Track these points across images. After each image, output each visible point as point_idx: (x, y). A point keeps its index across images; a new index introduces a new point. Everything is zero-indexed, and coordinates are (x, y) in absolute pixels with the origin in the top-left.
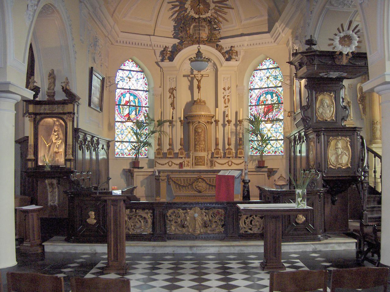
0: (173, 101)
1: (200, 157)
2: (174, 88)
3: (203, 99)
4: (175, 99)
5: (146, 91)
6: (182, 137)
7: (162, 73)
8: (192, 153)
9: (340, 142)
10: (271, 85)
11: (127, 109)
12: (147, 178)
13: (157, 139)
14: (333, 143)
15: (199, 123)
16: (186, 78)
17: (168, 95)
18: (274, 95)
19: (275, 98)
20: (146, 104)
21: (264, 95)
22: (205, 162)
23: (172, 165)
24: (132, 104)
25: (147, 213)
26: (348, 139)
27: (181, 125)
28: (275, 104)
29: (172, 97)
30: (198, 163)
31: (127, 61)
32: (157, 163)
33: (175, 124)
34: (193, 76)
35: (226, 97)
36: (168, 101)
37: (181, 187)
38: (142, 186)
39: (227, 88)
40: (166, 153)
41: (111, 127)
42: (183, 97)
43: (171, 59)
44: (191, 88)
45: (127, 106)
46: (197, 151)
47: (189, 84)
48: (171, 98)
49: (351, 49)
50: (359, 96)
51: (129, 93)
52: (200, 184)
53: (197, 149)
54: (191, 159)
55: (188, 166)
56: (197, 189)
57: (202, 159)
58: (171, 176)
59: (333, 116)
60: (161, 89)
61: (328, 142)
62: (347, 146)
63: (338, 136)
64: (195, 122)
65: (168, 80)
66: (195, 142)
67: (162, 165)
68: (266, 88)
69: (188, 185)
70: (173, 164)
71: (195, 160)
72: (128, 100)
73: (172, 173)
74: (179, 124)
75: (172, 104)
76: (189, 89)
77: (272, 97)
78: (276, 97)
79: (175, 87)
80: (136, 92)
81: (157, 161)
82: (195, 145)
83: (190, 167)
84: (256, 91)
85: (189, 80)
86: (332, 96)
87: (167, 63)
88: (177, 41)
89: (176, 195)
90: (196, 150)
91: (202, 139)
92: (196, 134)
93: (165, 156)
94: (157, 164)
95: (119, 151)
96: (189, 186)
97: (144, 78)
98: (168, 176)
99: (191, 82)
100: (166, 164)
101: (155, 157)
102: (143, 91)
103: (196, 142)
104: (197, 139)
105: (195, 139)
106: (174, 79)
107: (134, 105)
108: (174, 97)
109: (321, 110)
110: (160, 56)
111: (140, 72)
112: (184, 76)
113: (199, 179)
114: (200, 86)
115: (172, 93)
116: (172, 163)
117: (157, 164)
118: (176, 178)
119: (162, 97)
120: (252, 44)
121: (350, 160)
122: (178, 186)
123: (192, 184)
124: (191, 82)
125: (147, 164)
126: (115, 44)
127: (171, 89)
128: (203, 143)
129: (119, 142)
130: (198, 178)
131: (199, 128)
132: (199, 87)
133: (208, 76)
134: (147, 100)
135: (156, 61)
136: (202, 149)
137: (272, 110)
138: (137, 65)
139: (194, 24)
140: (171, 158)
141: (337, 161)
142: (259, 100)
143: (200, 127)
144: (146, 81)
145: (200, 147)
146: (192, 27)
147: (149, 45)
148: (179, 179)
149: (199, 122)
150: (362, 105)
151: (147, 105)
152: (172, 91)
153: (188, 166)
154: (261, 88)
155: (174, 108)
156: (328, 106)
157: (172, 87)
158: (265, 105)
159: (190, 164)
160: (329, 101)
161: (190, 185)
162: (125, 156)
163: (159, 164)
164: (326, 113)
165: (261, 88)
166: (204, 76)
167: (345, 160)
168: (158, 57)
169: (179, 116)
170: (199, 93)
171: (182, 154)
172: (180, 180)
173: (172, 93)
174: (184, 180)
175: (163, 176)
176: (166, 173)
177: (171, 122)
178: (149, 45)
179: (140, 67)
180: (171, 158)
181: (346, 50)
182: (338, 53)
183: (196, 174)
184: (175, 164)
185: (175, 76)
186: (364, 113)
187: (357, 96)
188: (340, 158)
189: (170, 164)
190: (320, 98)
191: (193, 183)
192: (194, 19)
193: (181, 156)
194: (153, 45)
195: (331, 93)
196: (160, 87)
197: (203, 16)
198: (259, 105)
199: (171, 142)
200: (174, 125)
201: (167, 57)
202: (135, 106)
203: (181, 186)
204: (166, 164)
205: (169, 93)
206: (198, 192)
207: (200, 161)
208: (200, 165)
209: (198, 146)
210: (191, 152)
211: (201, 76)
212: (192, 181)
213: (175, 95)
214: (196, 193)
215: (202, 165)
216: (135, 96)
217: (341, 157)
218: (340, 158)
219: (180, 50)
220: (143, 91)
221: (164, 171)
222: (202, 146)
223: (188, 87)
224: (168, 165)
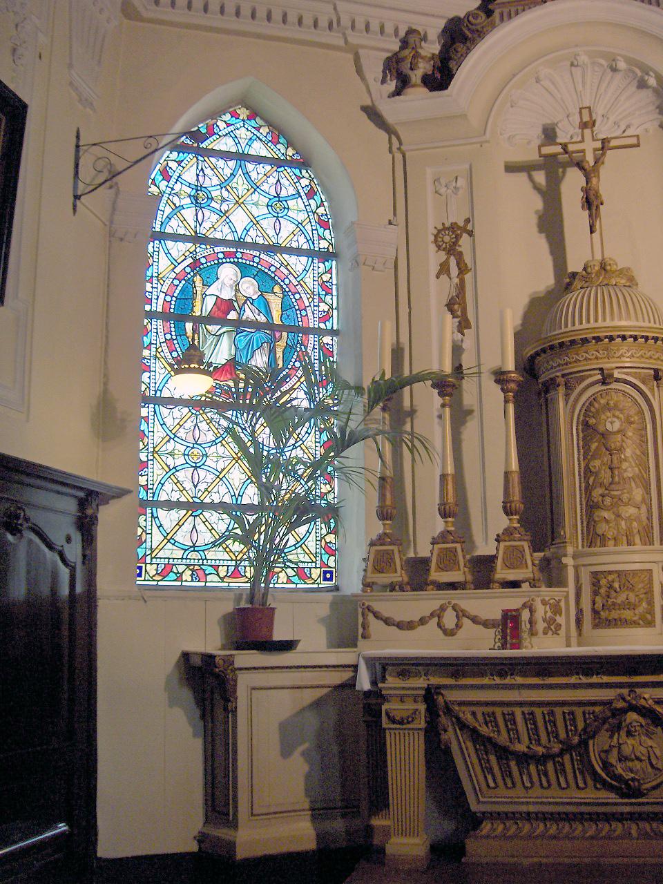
0: (461, 287)
1: (619, 573)
2: (461, 224)
3: (620, 257)
4: (468, 277)
5: (325, 256)
6: (514, 466)
7: (399, 156)
8: (574, 557)
11: (225, 338)
12: (317, 704)
13: (376, 483)
15: (604, 382)
16: (523, 176)
17: (435, 258)
20: (326, 317)
22: (651, 603)
23: (458, 626)
24: (248, 314)
27: (506, 401)
29: (454, 271)
30: (614, 614)
31: (227, 117)
32: (377, 615)
33: (476, 408)
34: (558, 149)
36: (436, 291)
37: (513, 764)
38: (286, 752)
40: (425, 562)
41: (115, 419)
42: (513, 271)
43: (440, 79)
44: (551, 224)
45: (224, 322)
46: (604, 540)
47: (538, 203)
48: (448, 273)
51: (234, 263)
52: (629, 745)
53: (602, 528)
54: (571, 588)
55: (556, 633)
56: (618, 778)
57: (632, 589)
58: (453, 696)
60: (397, 232)
64: (583, 379)
65: (430, 188)
66: (588, 490)
67: (400, 626)
69: (556, 748)
70: (466, 622)
71: (595, 593)
72: (227, 294)
73: (455, 675)
74: (494, 394)
75: (455, 305)
76: (541, 231)
79: (467, 221)
80: (275, 260)
81: (377, 606)
82: (591, 507)
83: (568, 638)
85: (536, 187)
87: (418, 99)
89: (483, 808)
90: (593, 538)
91: (629, 469)
92: (594, 446)
93: (418, 576)
94: (375, 625)
95: (179, 554)
96: (567, 758)
97: (311, 194)
98: (429, 696)
99: (551, 197)
100: (423, 621)
101: (367, 585)
102: (310, 253)
103: (597, 492)
104: (597, 474)
105: (588, 472)
106: (462, 182)
107: (262, 319)
108: (463, 269)
110: (383, 81)
112: (511, 168)
113: (624, 711)
114: (597, 195)
115: (452, 250)
116: (461, 614)
117: (375, 625)
118: (479, 710)
119: (401, 271)
122: (493, 758)
123: (584, 743)
124: (551, 197)
125: (322, 621)
126: (145, 14)
127: (444, 229)
128: (638, 494)
129: (178, 505)
130: (621, 704)
131: (607, 407)
132: (591, 202)
133: (634, 141)
134: (332, 300)
135: (368, 102)
136: (629, 528)
138: (278, 132)
140: (452, 586)
143: (616, 407)
144: (321, 211)
145: (618, 516)
147: (323, 23)
148: (498, 711)
149: (606, 379)
151: (334, 323)
152: (452, 239)
153: (556, 633)
155: (463, 325)
157: (452, 220)
159: (566, 620)
161: (567, 748)
162: (213, 581)
163: (387, 621)
166: (613, 143)
168: (375, 86)
169: (491, 362)
170: (592, 232)
171: (515, 560)
172: (510, 720)
173: (452, 250)
174: (530, 718)
175: (402, 701)
176: (418, 675)
177: (447, 386)
178: (323, 23)
179: (289, 144)
180: (452, 586)
183: (606, 679)
184: (475, 620)
185: (467, 166)
189: (449, 619)
191: (589, 734)
193: (511, 575)
194: (346, 22)
196: (390, 223)
199: (451, 499)
200: (470, 412)
201: (416, 77)
202: (269, 326)
203: (514, 753)
204: (423, 621)
205: (439, 247)
206: (623, 796)
207: (621, 598)
208: (626, 623)
209: (605, 514)
210: (570, 550)
211: (599, 145)
212: (581, 725)
213: (468, 259)
214: (612, 797)
215: (634, 624)
216: (266, 279)
219: (480, 34)
220: (310, 253)
221: (406, 667)
222: (632, 511)
223: (534, 220)
224: (439, 626)
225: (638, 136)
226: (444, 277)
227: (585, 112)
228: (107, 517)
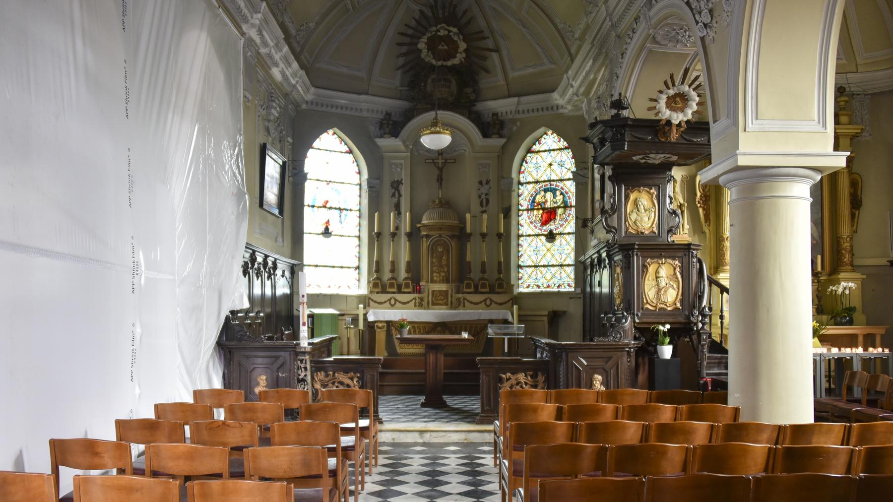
10: (554, 177)
14: (651, 269)
18: (558, 193)
19: (559, 198)
21: (542, 193)
25: (352, 379)
26: (677, 262)
28: (559, 207)
35: (483, 196)
39: (484, 182)
49: (685, 115)
50: (699, 194)
62: (675, 274)
63: (660, 257)
68: (545, 181)
77: (555, 196)
78: (561, 197)
84: (530, 187)
86: (652, 194)
100: (385, 302)
109: (634, 217)
111: (347, 152)
116: (396, 300)
117: (372, 303)
120: (526, 110)
121: (680, 297)
137: (555, 218)
139: (434, 76)
140: (394, 293)
141: (658, 298)
142: (534, 201)
146: (429, 81)
150: (704, 209)
154: (537, 182)
156: (645, 211)
158: (542, 209)
163: (375, 302)
164: (642, 221)
165: (537, 182)
167: (672, 297)
181: (677, 118)
182: (663, 122)
184: (400, 302)
186: (706, 222)
187: (696, 195)
189: (393, 302)
190: (632, 197)
192: (432, 68)
197: (449, 63)
198: (532, 210)
204: (385, 302)
217: (665, 292)
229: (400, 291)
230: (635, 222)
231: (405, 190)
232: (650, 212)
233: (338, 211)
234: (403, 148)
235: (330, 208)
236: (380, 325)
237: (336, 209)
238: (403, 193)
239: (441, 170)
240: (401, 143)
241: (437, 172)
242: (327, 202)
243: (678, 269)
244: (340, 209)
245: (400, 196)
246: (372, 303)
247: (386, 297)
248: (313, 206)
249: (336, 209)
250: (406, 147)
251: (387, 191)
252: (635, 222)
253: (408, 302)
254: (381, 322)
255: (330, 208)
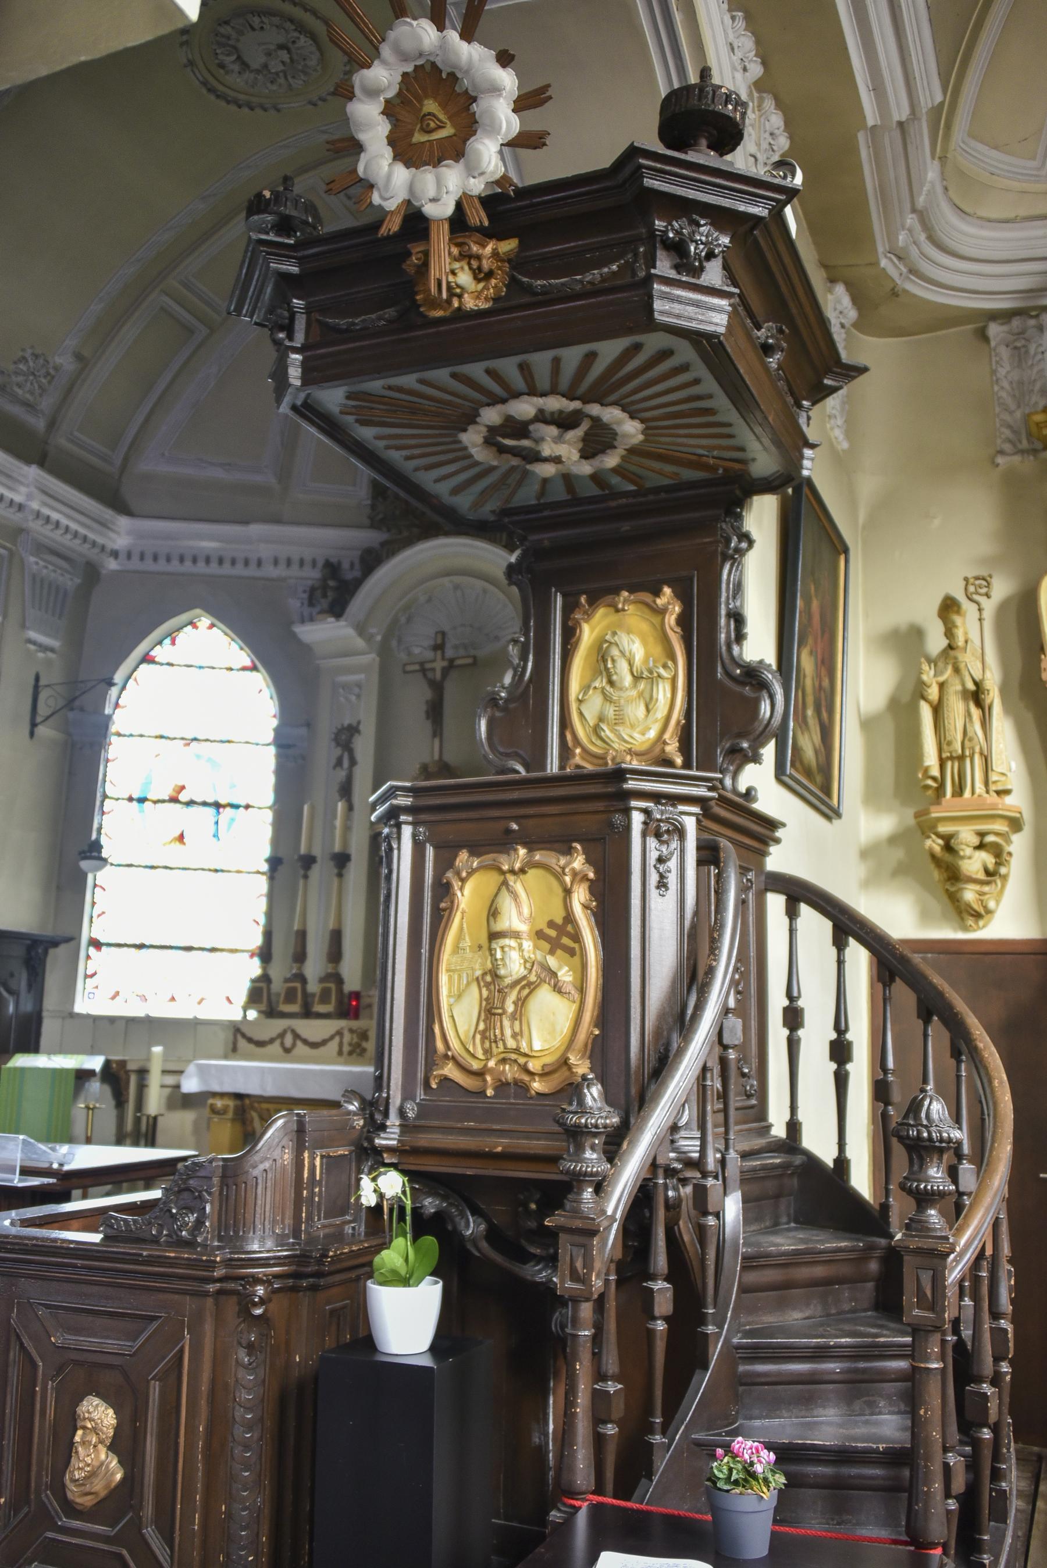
9: (519, 887)
14: (468, 896)
23: (294, 1045)
26: (578, 862)
29: (346, 763)
32: (244, 1036)
59: (667, 736)
61: (443, 890)
62: (569, 918)
63: (505, 843)
70: (299, 1043)
86: (662, 612)
88: (371, 537)
100: (272, 1041)
116: (296, 1036)
156: (637, 678)
160: (645, 643)
164: (619, 719)
167: (551, 1026)
184: (305, 1042)
188: (510, 1008)
189: (289, 1040)
190: (587, 635)
195: (657, 593)
204: (272, 1041)
217: (521, 1003)
218: (510, 1008)
225: (475, 657)
226: (338, 769)
227: (439, 637)
228: (56, 957)
229: (307, 1013)
230: (596, 730)
231: (364, 747)
232: (653, 679)
233: (211, 811)
234: (360, 643)
235: (191, 803)
236: (219, 1103)
237: (205, 804)
238: (359, 756)
239: (437, 687)
240: (350, 632)
241: (428, 694)
242: (183, 788)
243: (580, 895)
244: (217, 806)
245: (353, 762)
246: (242, 1043)
247: (280, 1024)
248: (142, 800)
249: (205, 804)
250: (369, 639)
251: (325, 751)
252: (596, 730)
253: (324, 1043)
254: (222, 1095)
255: (191, 803)
